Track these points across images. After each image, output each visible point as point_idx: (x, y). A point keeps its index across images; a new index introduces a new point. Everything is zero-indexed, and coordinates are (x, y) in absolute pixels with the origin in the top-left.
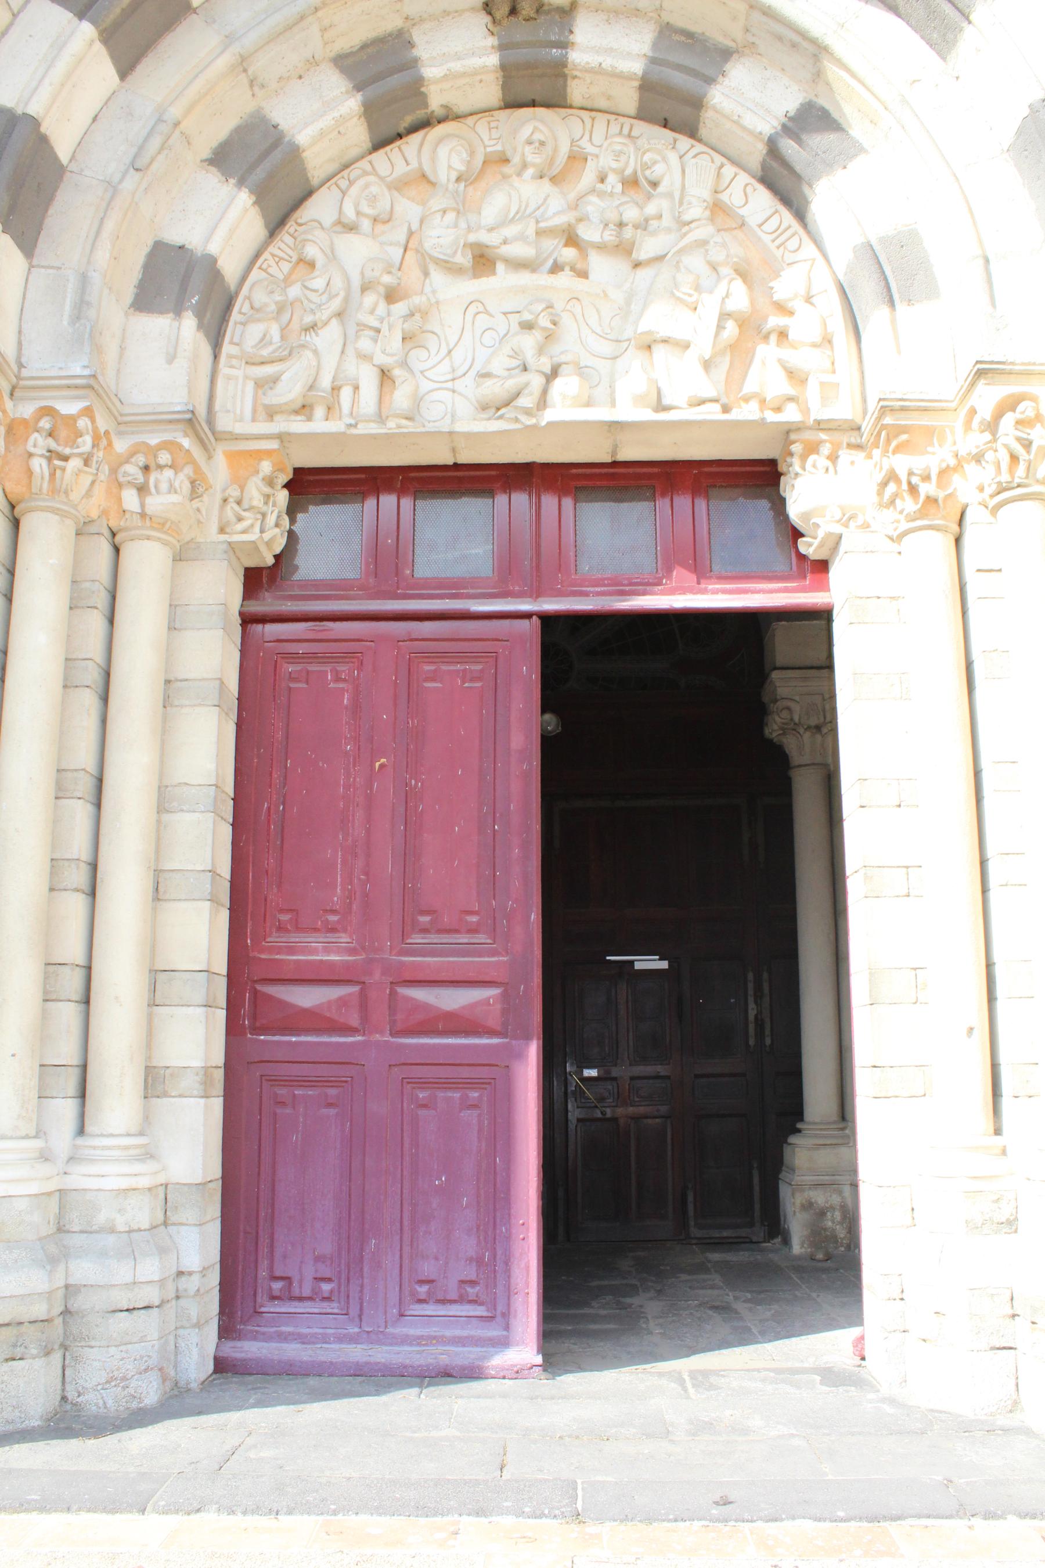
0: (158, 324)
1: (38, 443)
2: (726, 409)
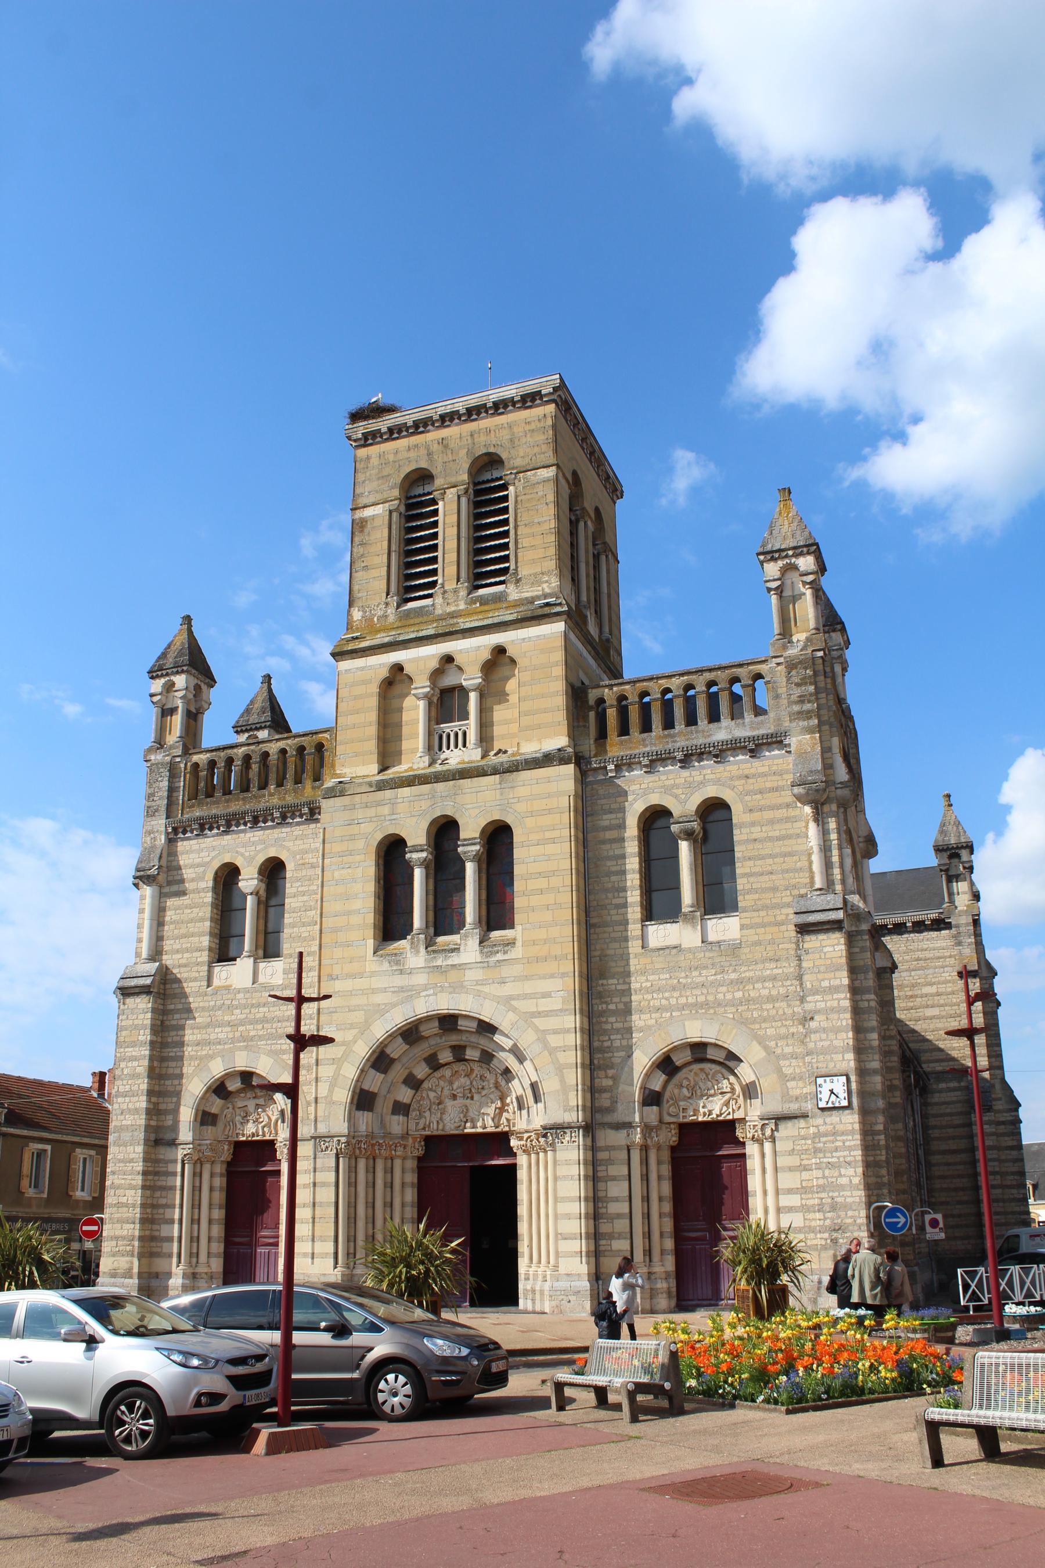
0: (396, 1117)
1: (376, 1147)
2: (497, 1127)
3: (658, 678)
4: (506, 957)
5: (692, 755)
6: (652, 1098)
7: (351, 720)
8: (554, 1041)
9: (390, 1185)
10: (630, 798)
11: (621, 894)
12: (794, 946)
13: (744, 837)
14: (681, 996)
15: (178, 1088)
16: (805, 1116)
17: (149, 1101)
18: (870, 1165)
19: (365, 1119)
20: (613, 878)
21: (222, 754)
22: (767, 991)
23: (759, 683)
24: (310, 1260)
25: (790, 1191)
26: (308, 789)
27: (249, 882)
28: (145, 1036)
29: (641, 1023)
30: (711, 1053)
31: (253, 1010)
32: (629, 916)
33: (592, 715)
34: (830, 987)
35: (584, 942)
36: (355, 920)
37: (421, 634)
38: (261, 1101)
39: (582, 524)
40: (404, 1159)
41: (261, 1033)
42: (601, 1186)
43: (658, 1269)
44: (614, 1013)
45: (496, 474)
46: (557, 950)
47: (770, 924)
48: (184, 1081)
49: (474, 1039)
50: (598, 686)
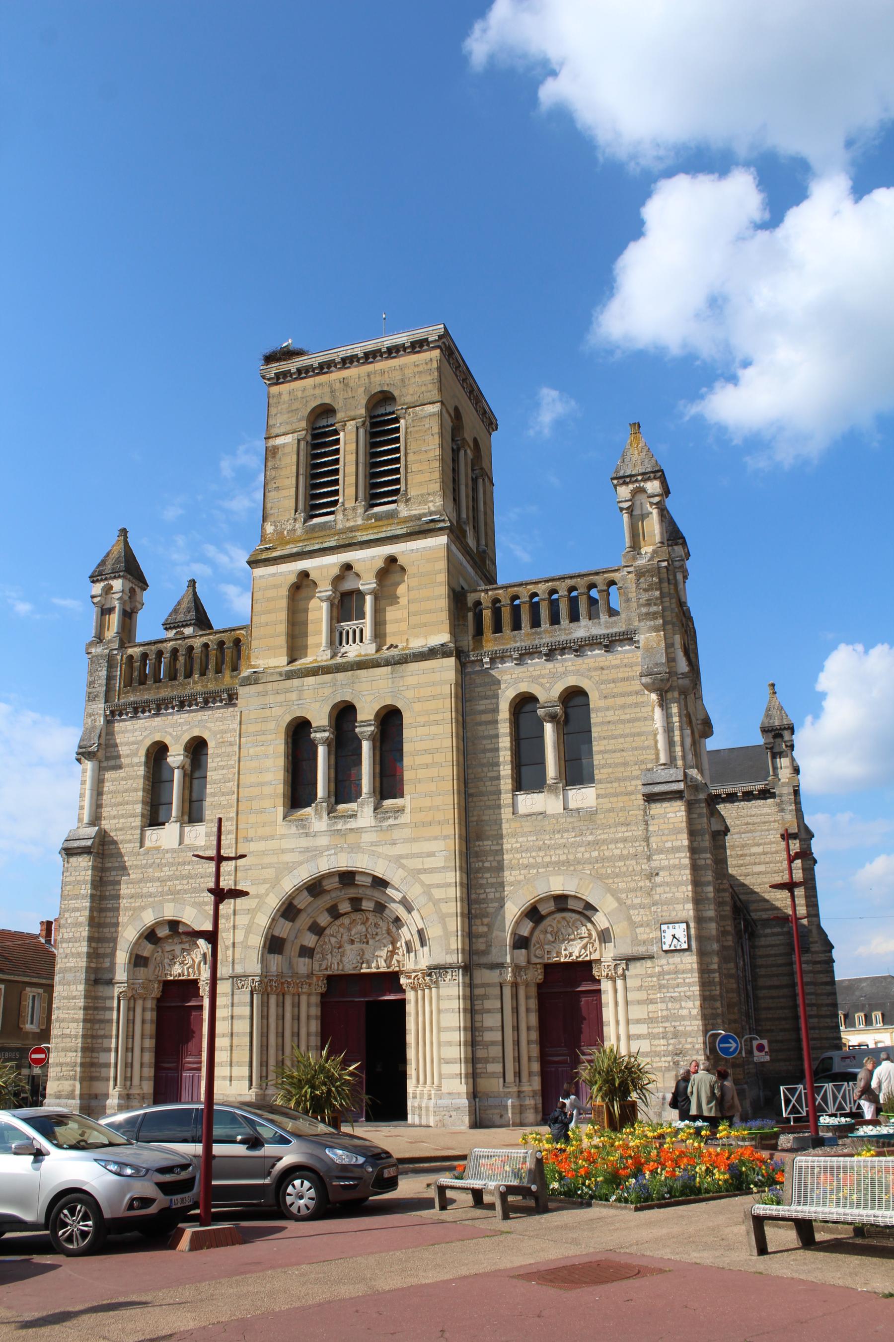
0: (302, 959)
1: (285, 985)
2: (388, 968)
3: (527, 584)
4: (397, 822)
5: (555, 649)
6: (521, 943)
7: (264, 619)
8: (438, 893)
9: (297, 1018)
10: (503, 686)
11: (495, 769)
12: (642, 812)
13: (599, 720)
14: (546, 855)
15: (114, 935)
16: (651, 957)
17: (89, 946)
18: (706, 999)
19: (275, 961)
20: (488, 755)
21: (153, 648)
22: (619, 851)
23: (613, 589)
24: (228, 1082)
25: (638, 1021)
26: (227, 678)
27: (176, 757)
28: (86, 890)
29: (512, 879)
30: (571, 904)
31: (179, 868)
32: (502, 787)
33: (470, 615)
34: (672, 848)
35: (463, 809)
36: (267, 790)
37: (324, 545)
38: (186, 946)
39: (462, 453)
40: (309, 995)
41: (186, 887)
42: (478, 1017)
43: (526, 1088)
44: (488, 870)
45: (389, 409)
46: (440, 816)
47: (621, 794)
48: (120, 929)
49: (369, 892)
50: (475, 591)
